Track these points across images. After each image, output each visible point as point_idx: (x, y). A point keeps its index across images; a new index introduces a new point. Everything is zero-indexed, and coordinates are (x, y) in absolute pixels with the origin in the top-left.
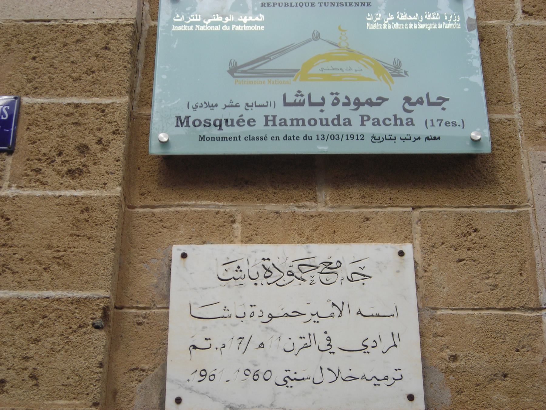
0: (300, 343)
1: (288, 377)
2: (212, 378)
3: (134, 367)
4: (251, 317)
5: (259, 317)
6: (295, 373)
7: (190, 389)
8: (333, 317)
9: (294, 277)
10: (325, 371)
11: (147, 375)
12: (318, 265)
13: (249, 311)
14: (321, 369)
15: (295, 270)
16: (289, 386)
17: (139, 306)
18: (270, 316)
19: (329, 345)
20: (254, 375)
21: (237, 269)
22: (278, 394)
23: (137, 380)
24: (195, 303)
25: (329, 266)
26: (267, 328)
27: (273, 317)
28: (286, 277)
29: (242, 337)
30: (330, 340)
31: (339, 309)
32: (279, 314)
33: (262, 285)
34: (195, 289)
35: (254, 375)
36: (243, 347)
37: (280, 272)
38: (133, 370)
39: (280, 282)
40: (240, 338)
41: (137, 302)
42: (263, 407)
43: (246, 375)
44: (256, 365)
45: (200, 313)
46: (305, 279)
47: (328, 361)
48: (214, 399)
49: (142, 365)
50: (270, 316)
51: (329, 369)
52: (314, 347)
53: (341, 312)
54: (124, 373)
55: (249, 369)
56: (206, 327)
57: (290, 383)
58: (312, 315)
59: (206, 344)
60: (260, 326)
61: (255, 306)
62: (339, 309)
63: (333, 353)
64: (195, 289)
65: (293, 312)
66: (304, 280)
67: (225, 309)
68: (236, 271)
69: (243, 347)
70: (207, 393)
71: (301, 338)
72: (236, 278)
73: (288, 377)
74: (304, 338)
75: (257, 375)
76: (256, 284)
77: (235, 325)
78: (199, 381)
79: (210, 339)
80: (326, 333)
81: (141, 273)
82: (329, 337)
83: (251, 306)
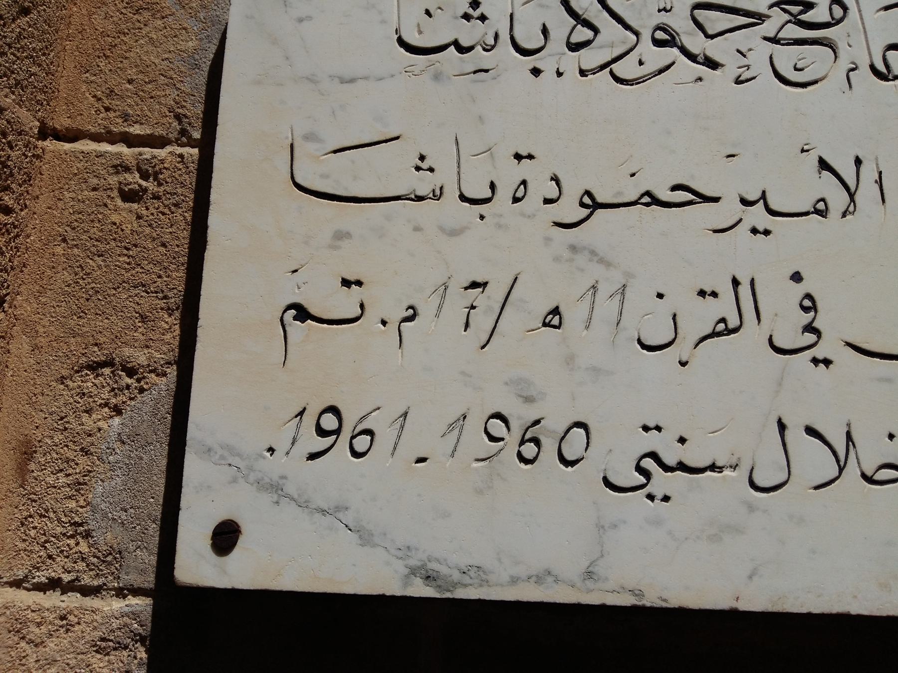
0: (701, 317)
1: (653, 455)
2: (362, 443)
3: (98, 355)
4: (516, 200)
5: (547, 201)
6: (682, 440)
7: (275, 489)
8: (823, 213)
9: (675, 51)
10: (796, 436)
11: (142, 390)
12: (763, 10)
13: (509, 176)
14: (782, 427)
15: (680, 22)
16: (660, 495)
17: (131, 130)
18: (587, 200)
19: (809, 328)
20: (522, 442)
21: (470, 11)
22: (615, 526)
23: (106, 405)
24: (310, 137)
25: (803, 17)
26: (573, 248)
27: (597, 206)
28: (646, 47)
29: (479, 280)
30: (814, 308)
31: (844, 183)
32: (619, 193)
33: (559, 74)
34: (311, 79)
35: (522, 442)
36: (482, 322)
37: (627, 27)
38: (95, 367)
39: (622, 69)
40: (474, 285)
41: (126, 117)
42: (556, 581)
43: (492, 439)
44: (529, 400)
45: (325, 176)
46: (717, 58)
47: (816, 395)
48: (364, 536)
49: (127, 351)
50: (587, 200)
51: (811, 431)
52: (753, 336)
53: (852, 196)
54: (62, 380)
55: (504, 413)
56: (348, 235)
57: (661, 482)
58: (745, 202)
59: (344, 304)
60: (548, 240)
61: (530, 157)
62: (844, 183)
63: (827, 362)
64: (311, 79)
65: (674, 188)
66: (712, 64)
67: (422, 164)
68: (467, 17)
69: (482, 322)
70: (338, 509)
71: (702, 293)
72: (465, 43)
73: (653, 455)
74: (714, 294)
75: (536, 441)
76: (536, 72)
77: (454, 233)
78: (313, 456)
79: (359, 283)
80: (797, 277)
81: (147, 14)
82: (808, 296)
83: (518, 157)
